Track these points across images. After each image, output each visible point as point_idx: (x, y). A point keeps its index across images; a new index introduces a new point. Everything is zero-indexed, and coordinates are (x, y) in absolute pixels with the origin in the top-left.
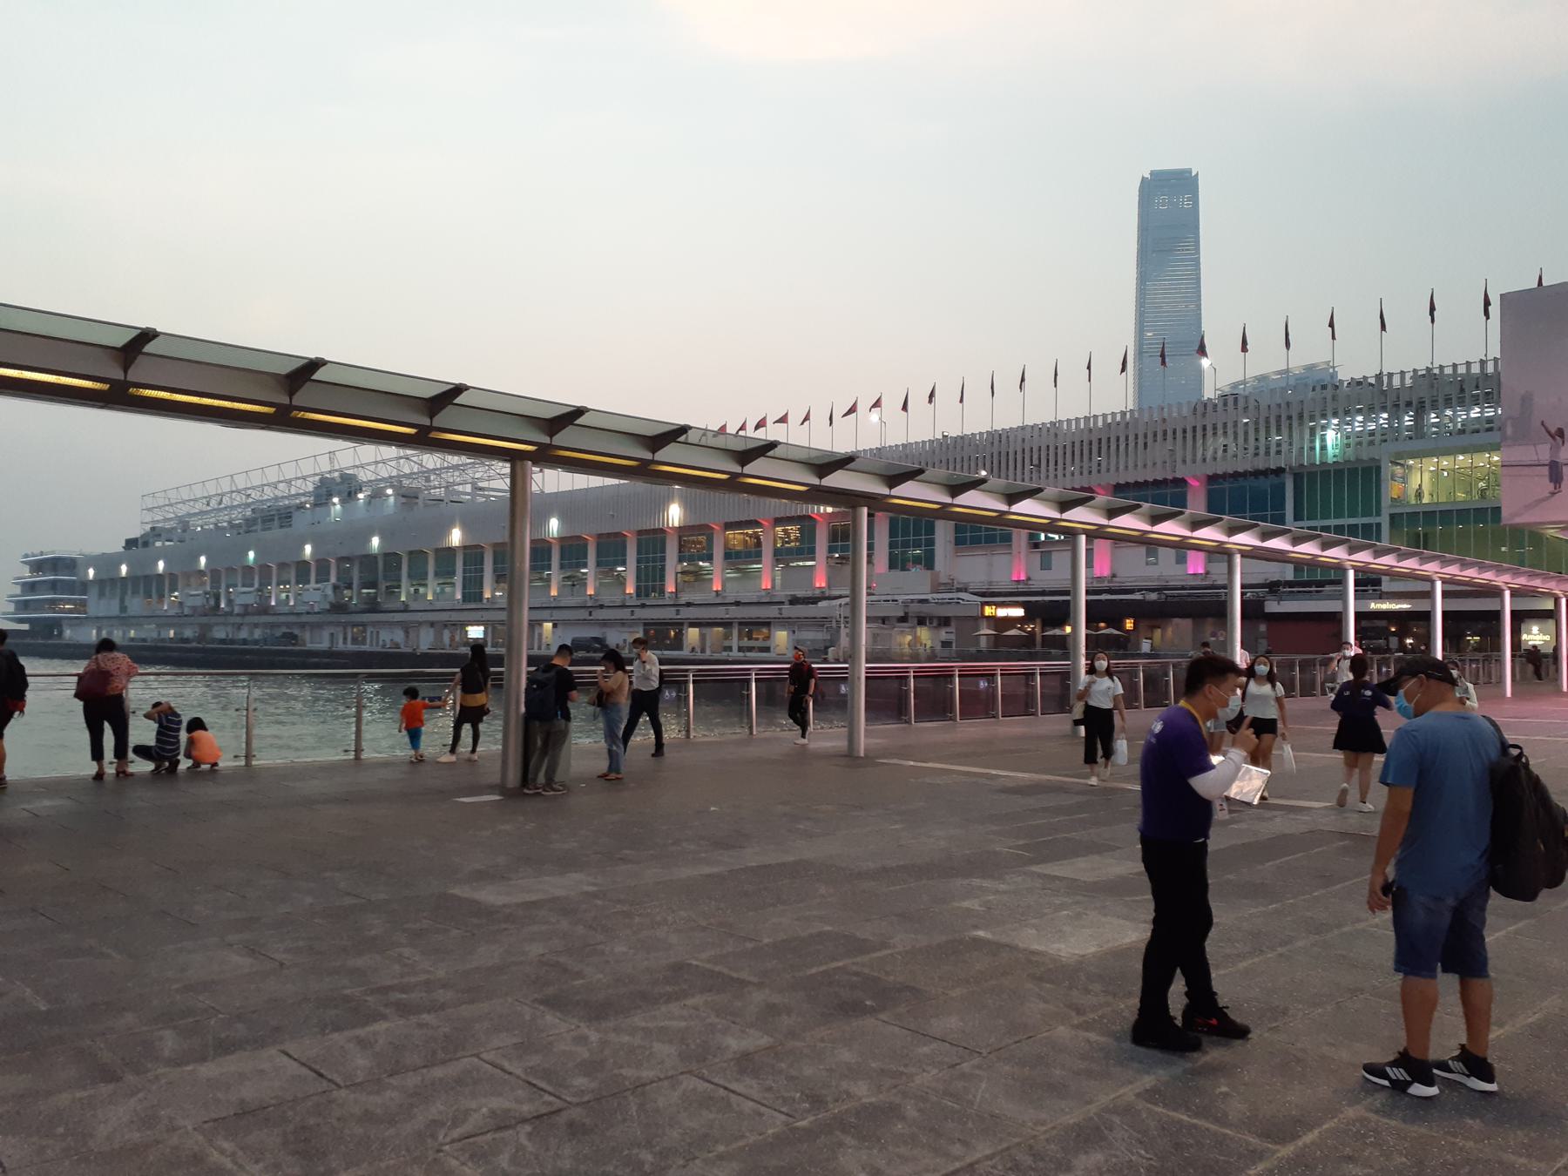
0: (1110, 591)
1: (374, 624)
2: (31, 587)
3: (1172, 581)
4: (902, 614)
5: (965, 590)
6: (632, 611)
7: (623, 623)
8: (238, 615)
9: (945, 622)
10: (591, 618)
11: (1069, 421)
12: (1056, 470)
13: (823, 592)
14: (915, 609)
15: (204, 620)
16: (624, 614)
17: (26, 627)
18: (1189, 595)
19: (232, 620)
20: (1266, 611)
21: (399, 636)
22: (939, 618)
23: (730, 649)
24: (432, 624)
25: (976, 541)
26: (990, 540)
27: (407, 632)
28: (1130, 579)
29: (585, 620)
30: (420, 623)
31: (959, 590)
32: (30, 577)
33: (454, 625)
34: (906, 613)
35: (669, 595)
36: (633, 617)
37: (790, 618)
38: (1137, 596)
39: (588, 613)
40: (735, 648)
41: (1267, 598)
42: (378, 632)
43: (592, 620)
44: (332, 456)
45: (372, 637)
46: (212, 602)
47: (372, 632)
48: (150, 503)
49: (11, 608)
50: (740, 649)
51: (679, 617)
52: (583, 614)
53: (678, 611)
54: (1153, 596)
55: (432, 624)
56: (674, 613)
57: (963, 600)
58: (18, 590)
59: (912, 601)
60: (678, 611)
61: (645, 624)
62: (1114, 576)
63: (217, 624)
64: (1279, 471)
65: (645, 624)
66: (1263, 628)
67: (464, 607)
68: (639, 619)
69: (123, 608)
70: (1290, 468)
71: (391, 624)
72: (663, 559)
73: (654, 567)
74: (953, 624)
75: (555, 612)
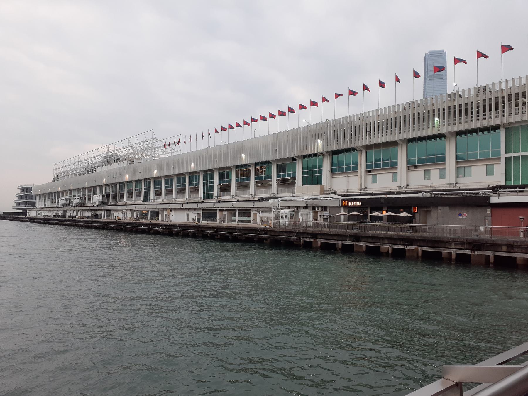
0: (405, 193)
1: (113, 210)
2: (21, 197)
3: (438, 187)
4: (305, 205)
5: (335, 193)
8: (74, 207)
9: (325, 208)
10: (183, 207)
11: (385, 108)
12: (379, 133)
13: (274, 196)
14: (309, 203)
15: (64, 209)
16: (195, 206)
17: (21, 211)
18: (447, 194)
19: (71, 208)
20: (491, 202)
21: (120, 215)
22: (322, 207)
23: (234, 221)
24: (131, 210)
25: (341, 170)
26: (348, 169)
27: (123, 213)
28: (416, 187)
29: (181, 208)
30: (127, 210)
31: (332, 193)
32: (21, 194)
33: (137, 210)
34: (307, 205)
36: (198, 207)
37: (258, 207)
38: (420, 195)
40: (237, 221)
41: (491, 195)
44: (108, 147)
45: (112, 215)
46: (68, 202)
48: (56, 167)
49: (16, 205)
50: (239, 221)
51: (214, 207)
52: (180, 206)
54: (428, 195)
55: (131, 210)
56: (213, 205)
57: (333, 198)
58: (17, 198)
59: (310, 199)
61: (203, 210)
62: (408, 185)
63: (68, 210)
64: (496, 128)
65: (203, 210)
66: (489, 211)
67: (146, 203)
68: (200, 208)
69: (45, 205)
70: (503, 124)
71: (118, 210)
73: (207, 186)
74: (328, 209)
75: (170, 205)
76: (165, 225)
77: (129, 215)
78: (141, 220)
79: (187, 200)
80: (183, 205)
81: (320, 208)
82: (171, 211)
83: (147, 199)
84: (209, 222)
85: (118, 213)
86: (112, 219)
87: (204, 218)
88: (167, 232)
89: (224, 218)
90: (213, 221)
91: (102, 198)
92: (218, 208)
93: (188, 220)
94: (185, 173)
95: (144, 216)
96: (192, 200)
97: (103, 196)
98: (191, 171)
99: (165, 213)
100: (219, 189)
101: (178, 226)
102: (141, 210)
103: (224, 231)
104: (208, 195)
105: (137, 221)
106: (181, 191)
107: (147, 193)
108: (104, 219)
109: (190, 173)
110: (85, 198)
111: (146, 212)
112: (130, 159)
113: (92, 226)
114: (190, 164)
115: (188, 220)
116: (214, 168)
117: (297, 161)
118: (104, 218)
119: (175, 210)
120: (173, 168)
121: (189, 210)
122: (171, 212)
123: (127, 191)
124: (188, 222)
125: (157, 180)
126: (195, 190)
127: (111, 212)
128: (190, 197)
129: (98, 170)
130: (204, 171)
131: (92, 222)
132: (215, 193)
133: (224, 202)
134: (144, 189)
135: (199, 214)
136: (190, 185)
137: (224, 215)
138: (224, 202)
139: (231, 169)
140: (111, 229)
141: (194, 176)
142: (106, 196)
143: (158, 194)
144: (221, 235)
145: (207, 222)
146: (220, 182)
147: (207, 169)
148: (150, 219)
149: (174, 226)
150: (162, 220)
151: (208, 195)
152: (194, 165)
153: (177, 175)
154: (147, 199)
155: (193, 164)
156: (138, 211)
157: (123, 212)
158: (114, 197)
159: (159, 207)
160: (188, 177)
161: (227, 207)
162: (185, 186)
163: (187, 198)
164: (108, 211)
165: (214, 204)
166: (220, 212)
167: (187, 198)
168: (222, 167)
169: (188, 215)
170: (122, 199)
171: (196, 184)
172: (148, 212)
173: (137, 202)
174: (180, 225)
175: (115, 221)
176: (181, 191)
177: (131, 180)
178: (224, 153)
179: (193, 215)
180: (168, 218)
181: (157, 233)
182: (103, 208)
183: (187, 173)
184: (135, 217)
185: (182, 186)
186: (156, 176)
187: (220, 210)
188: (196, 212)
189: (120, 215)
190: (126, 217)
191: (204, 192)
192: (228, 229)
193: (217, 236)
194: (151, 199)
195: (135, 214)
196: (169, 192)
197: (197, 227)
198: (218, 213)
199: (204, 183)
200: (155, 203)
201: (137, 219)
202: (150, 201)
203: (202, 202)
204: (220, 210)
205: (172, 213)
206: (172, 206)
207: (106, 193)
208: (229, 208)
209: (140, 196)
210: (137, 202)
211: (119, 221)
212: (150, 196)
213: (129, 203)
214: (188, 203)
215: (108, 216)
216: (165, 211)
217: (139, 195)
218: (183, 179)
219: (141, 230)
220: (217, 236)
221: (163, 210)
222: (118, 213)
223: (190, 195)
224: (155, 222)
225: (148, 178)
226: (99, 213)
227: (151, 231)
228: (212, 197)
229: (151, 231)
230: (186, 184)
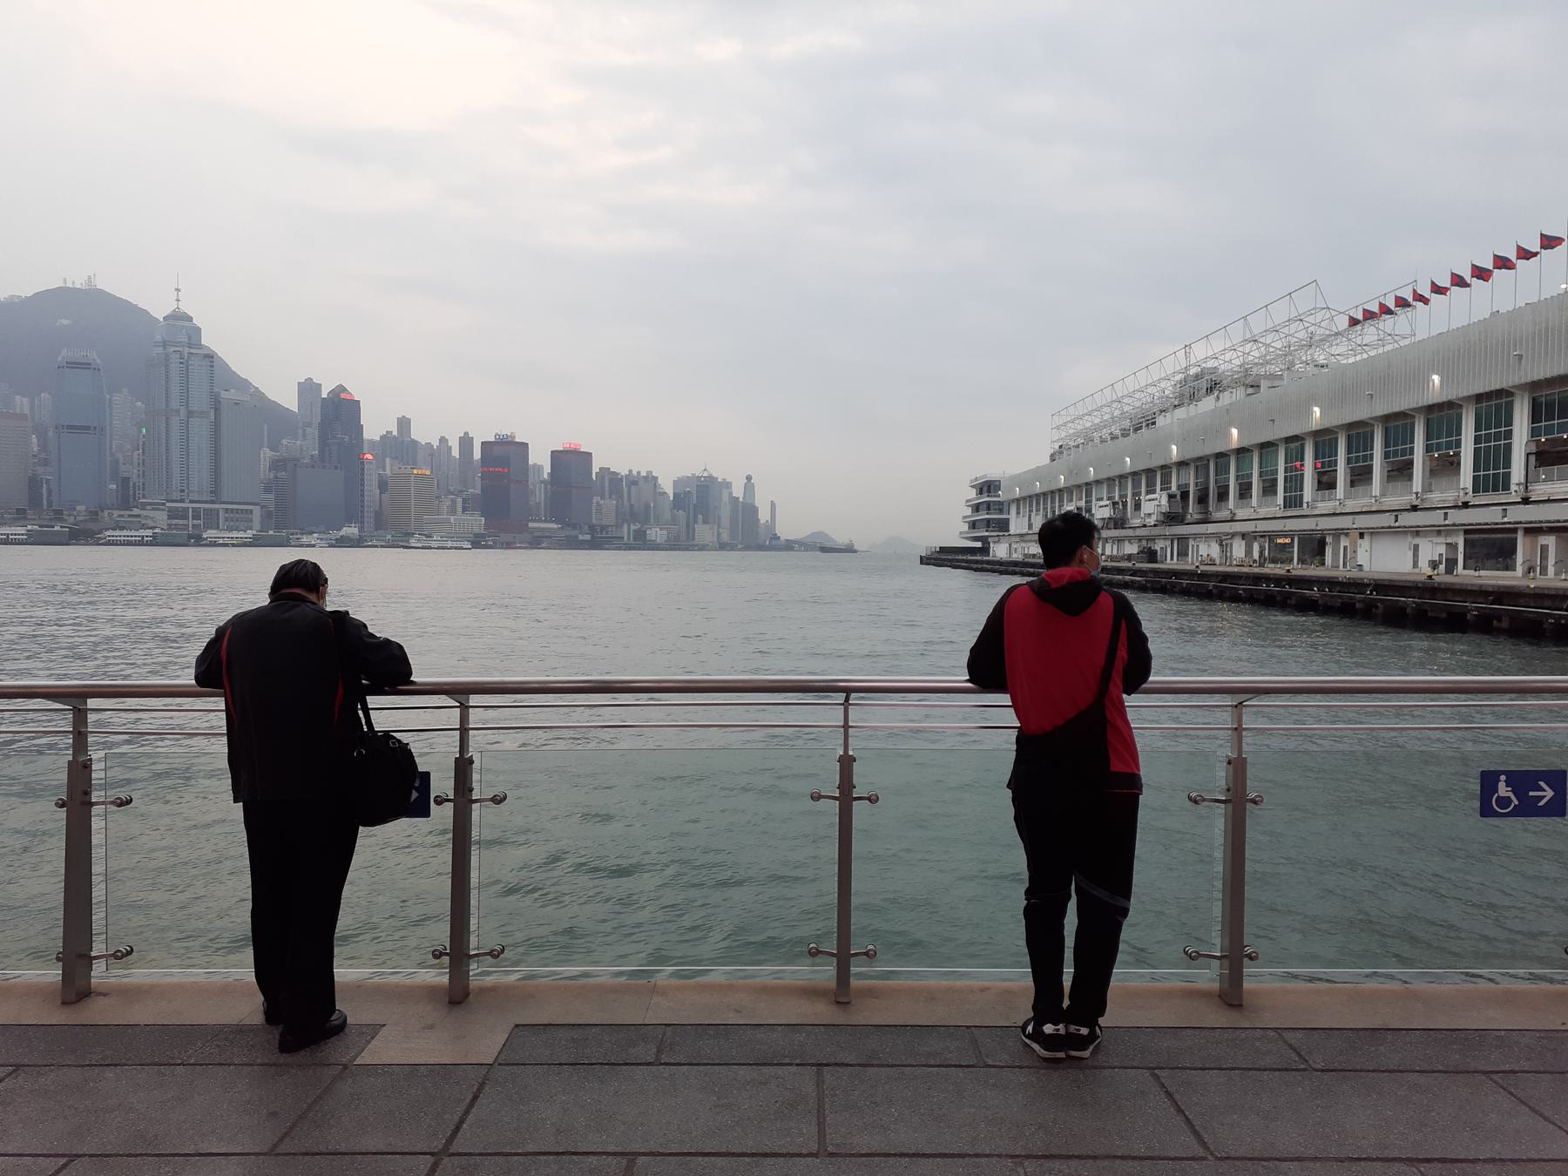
1: (1196, 536)
6: (1396, 521)
10: (1397, 524)
16: (1436, 518)
21: (1214, 550)
24: (1244, 536)
27: (1221, 545)
29: (1390, 527)
30: (1233, 535)
33: (1262, 536)
35: (1517, 488)
36: (1447, 522)
39: (1393, 518)
42: (1198, 546)
43: (1398, 527)
45: (1193, 549)
47: (1193, 546)
48: (1058, 421)
51: (1506, 520)
52: (1387, 520)
53: (1446, 514)
55: (1244, 536)
60: (1446, 514)
61: (1466, 532)
67: (1289, 514)
68: (1454, 525)
71: (1207, 537)
72: (1509, 435)
76: (1331, 583)
77: (1238, 550)
78: (1273, 565)
79: (1417, 498)
80: (1397, 516)
82: (1362, 536)
83: (1293, 501)
84: (1483, 573)
85: (1209, 546)
86: (1192, 563)
87: (1471, 558)
88: (1339, 604)
89: (1544, 557)
90: (1507, 569)
91: (1169, 501)
92: (1520, 523)
93: (1415, 564)
94: (1410, 410)
95: (1280, 553)
96: (1436, 497)
97: (1171, 496)
98: (1430, 403)
99: (1344, 542)
100: (1532, 459)
101: (1369, 585)
102: (1271, 536)
103: (1522, 601)
104: (1491, 477)
105: (1257, 570)
106: (1400, 470)
107: (1294, 482)
108: (1171, 563)
109: (1430, 409)
110: (1125, 505)
111: (1288, 541)
112: (1249, 381)
113: (1132, 581)
114: (1428, 380)
115: (1415, 564)
116: (1510, 384)
118: (1172, 558)
119: (1375, 532)
120: (1372, 395)
121: (1417, 532)
122: (1360, 541)
123: (1237, 478)
124: (1417, 570)
125: (1324, 440)
126: (1446, 465)
127: (1191, 542)
128: (1427, 488)
129: (1161, 421)
130: (1479, 398)
131: (1135, 573)
132: (1517, 472)
133: (1549, 501)
134: (1286, 470)
135: (1452, 547)
136: (1428, 449)
137: (1544, 549)
138: (1549, 501)
139: (1461, 406)
140: (1186, 593)
141: (1442, 416)
142: (1178, 497)
143: (1326, 483)
144: (1514, 616)
145: (1477, 574)
146: (1534, 433)
147: (1487, 390)
148: (1298, 564)
149: (1357, 585)
150: (1334, 565)
151: (1491, 477)
152: (1441, 382)
153: (1387, 419)
154: (1293, 501)
155: (1436, 378)
156: (1261, 539)
157: (1223, 541)
158: (1202, 499)
159: (1326, 524)
160: (1422, 421)
161: (1551, 519)
162: (1412, 453)
163: (1417, 493)
164: (1183, 540)
165: (1506, 510)
166: (1528, 539)
167: (1417, 493)
168: (1541, 376)
169: (1416, 548)
170: (1223, 504)
171: (1449, 446)
172: (1293, 540)
173: (1261, 511)
174: (1374, 580)
175: (1193, 568)
176: (1400, 470)
177: (1245, 444)
178: (1547, 328)
179: (1431, 550)
180: (1354, 558)
181: (1306, 606)
182: (1170, 531)
183: (1418, 410)
184: (1256, 555)
185: (1404, 453)
186: (1318, 428)
187: (1528, 531)
188: (1442, 540)
189: (1214, 550)
190: (1231, 556)
191: (1476, 468)
192: (1540, 597)
193: (1500, 620)
194: (1305, 500)
195: (1256, 547)
196: (1361, 476)
197: (1428, 589)
198: (1521, 542)
199: (1477, 440)
200: (1318, 510)
201: (1262, 561)
202: (1301, 506)
203: (1466, 505)
204: (1528, 531)
205: (1364, 544)
206: (1364, 522)
207: (1179, 487)
208: (1559, 521)
209: (1275, 493)
210: (1261, 511)
211: (1203, 568)
212: (1302, 490)
213: (1240, 514)
214: (1414, 508)
215: (1183, 553)
216: (1342, 537)
217: (1269, 489)
218: (1405, 426)
219: (1262, 597)
220: (1500, 620)
221: (1339, 533)
222: (1209, 546)
223: (1431, 484)
224: (1312, 571)
225: (1297, 436)
226: (1158, 546)
227: (1291, 599)
228: (1506, 487)
229: (1291, 599)
230: (1375, 452)
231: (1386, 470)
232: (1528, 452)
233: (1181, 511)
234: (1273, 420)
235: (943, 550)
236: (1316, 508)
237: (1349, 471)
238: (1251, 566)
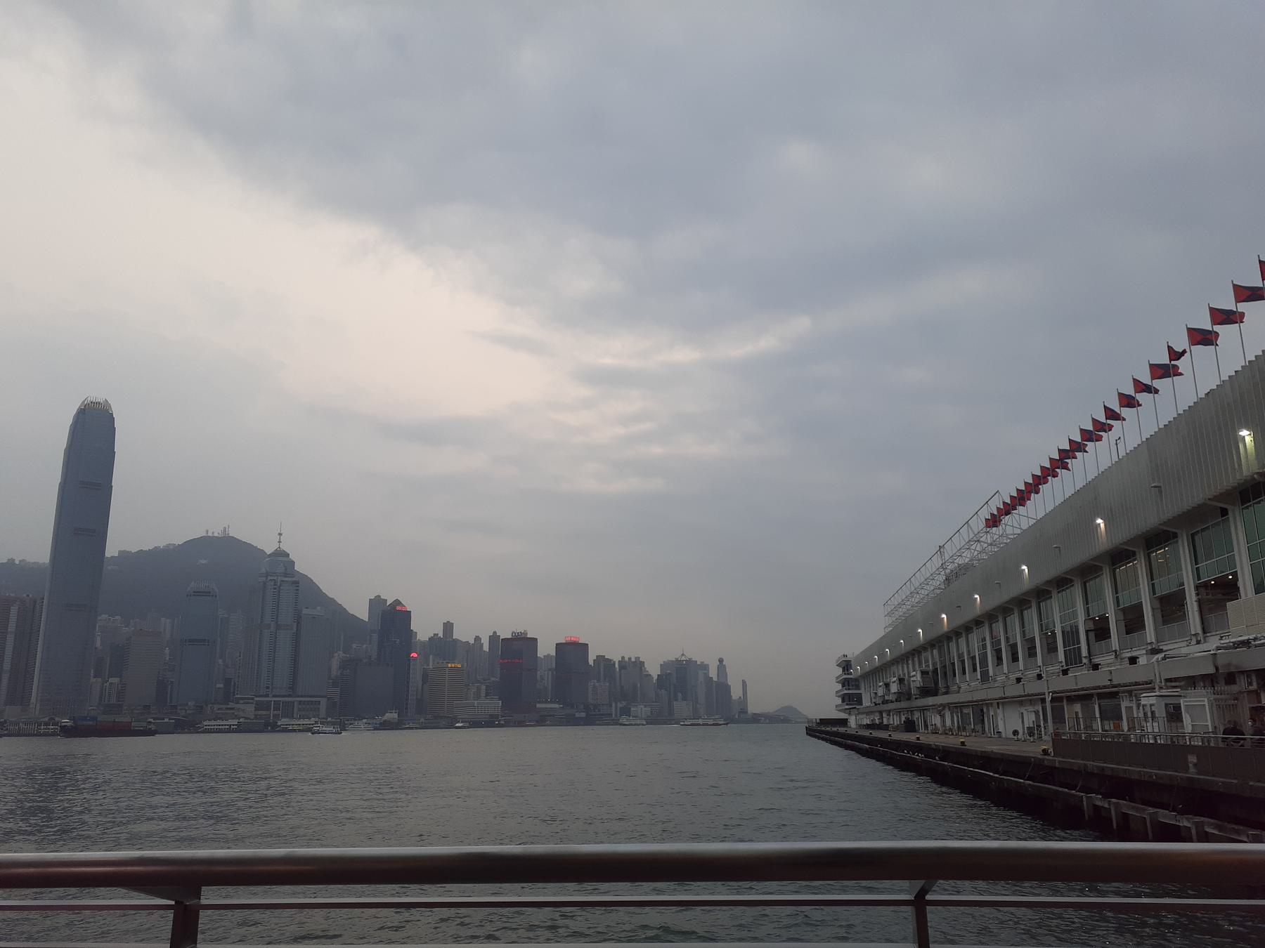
7: (1031, 700)
81: (1254, 678)
83: (985, 677)
91: (922, 677)
97: (924, 673)
100: (1092, 635)
117: (1230, 513)
231: (1026, 648)
232: (1087, 629)
233: (933, 685)
234: (960, 607)
235: (823, 722)
236: (996, 681)
237: (1009, 649)
238: (947, 734)
